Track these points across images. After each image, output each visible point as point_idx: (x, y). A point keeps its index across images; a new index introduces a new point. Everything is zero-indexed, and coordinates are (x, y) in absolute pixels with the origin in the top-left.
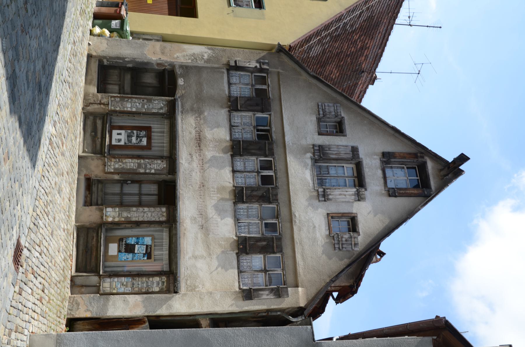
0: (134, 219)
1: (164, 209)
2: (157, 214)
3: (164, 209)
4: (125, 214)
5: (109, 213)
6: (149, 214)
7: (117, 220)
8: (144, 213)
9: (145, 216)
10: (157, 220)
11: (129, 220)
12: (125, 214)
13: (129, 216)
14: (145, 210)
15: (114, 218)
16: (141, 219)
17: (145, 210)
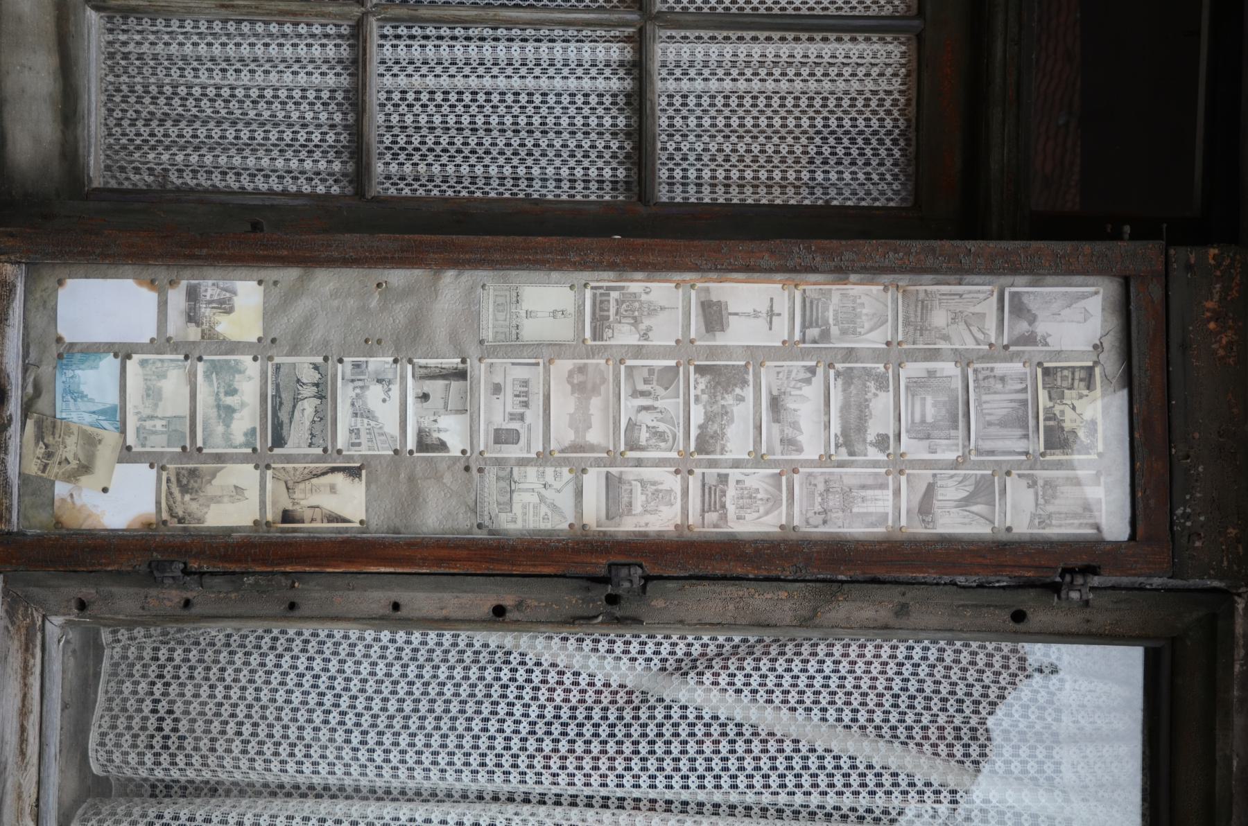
0: (538, 506)
1: (1076, 316)
2: (958, 415)
3: (1076, 316)
4: (382, 407)
5: (96, 381)
6: (811, 417)
7: (235, 503)
8: (722, 378)
9: (737, 442)
10: (955, 521)
11: (437, 516)
12: (382, 407)
13: (452, 430)
14: (742, 333)
15: (187, 469)
16: (660, 508)
17: (742, 333)
